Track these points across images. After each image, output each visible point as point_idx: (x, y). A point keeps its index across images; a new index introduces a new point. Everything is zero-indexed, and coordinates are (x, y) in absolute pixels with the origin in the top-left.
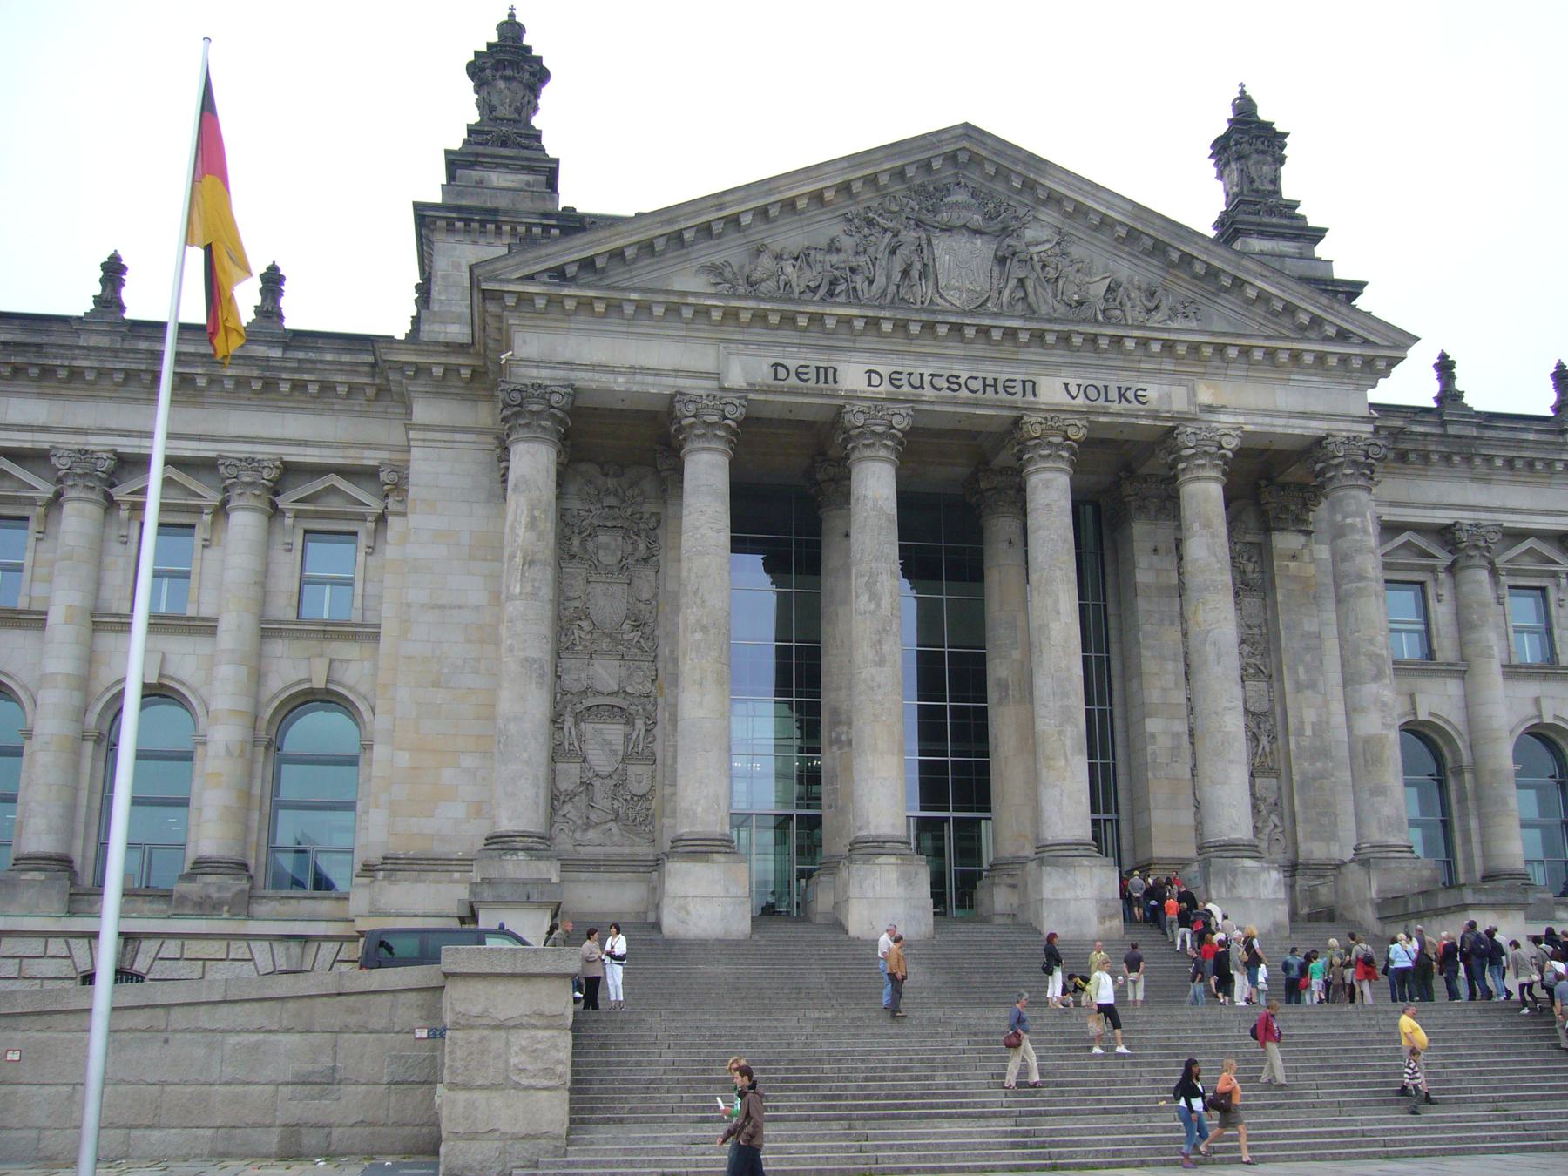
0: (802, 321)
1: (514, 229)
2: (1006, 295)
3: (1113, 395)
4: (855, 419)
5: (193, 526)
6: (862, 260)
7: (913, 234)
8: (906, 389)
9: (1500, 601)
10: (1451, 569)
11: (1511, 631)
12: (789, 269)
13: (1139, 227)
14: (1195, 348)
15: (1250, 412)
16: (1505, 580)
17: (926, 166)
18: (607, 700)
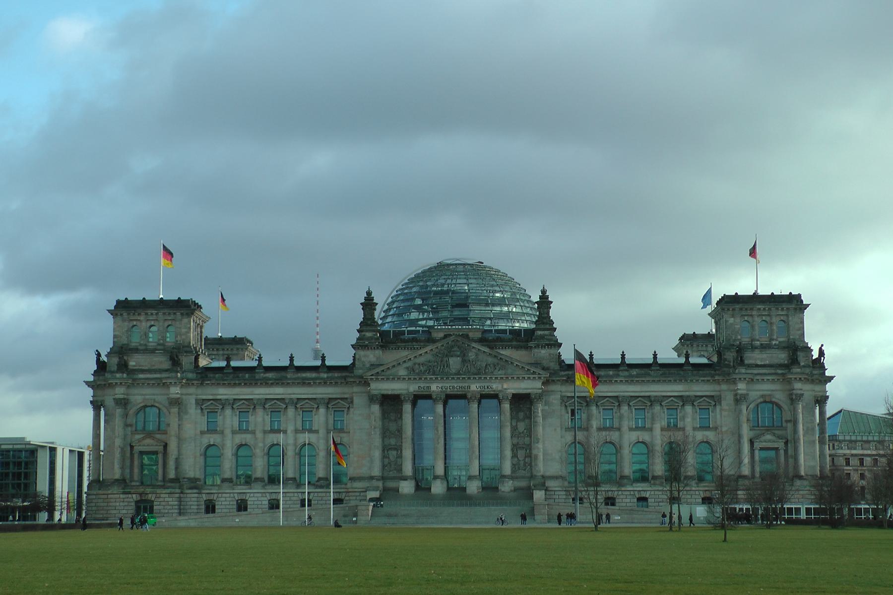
0: (423, 379)
1: (371, 348)
2: (464, 369)
3: (486, 387)
4: (434, 397)
5: (312, 411)
6: (435, 364)
7: (445, 359)
8: (444, 389)
9: (600, 412)
10: (587, 405)
11: (602, 419)
12: (421, 367)
13: (491, 353)
14: (502, 378)
15: (514, 389)
16: (601, 408)
17: (448, 343)
18: (393, 447)
